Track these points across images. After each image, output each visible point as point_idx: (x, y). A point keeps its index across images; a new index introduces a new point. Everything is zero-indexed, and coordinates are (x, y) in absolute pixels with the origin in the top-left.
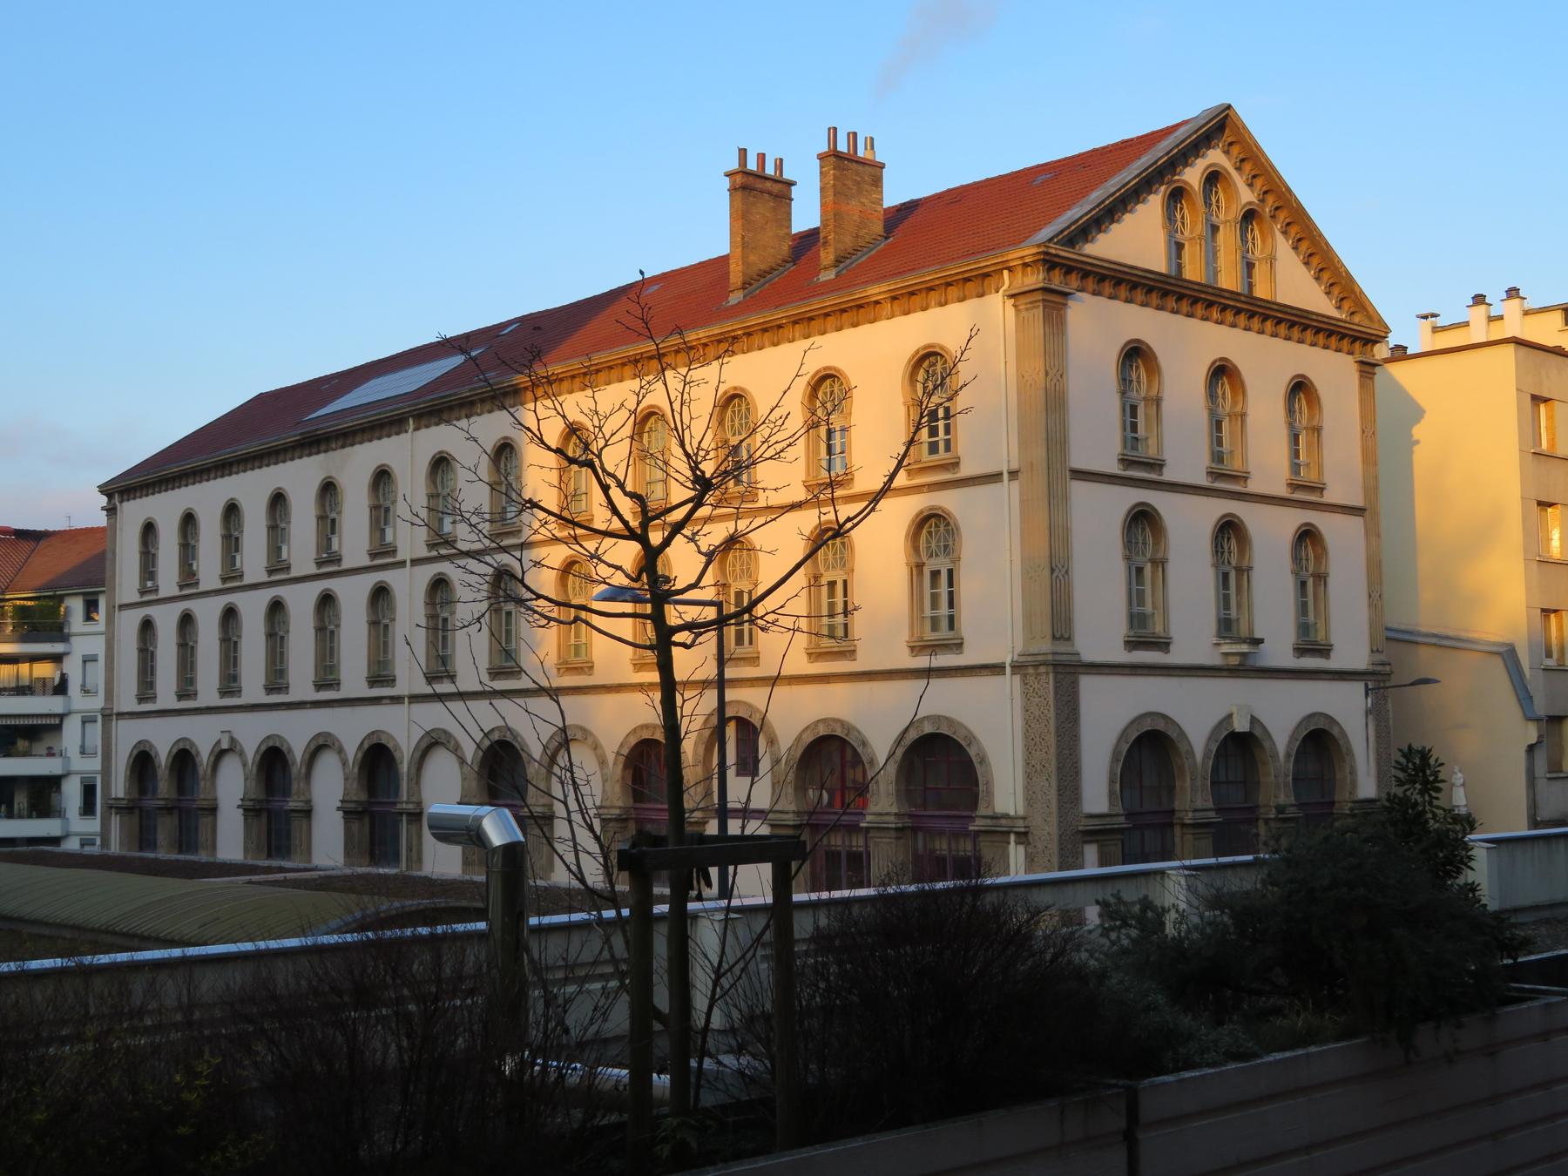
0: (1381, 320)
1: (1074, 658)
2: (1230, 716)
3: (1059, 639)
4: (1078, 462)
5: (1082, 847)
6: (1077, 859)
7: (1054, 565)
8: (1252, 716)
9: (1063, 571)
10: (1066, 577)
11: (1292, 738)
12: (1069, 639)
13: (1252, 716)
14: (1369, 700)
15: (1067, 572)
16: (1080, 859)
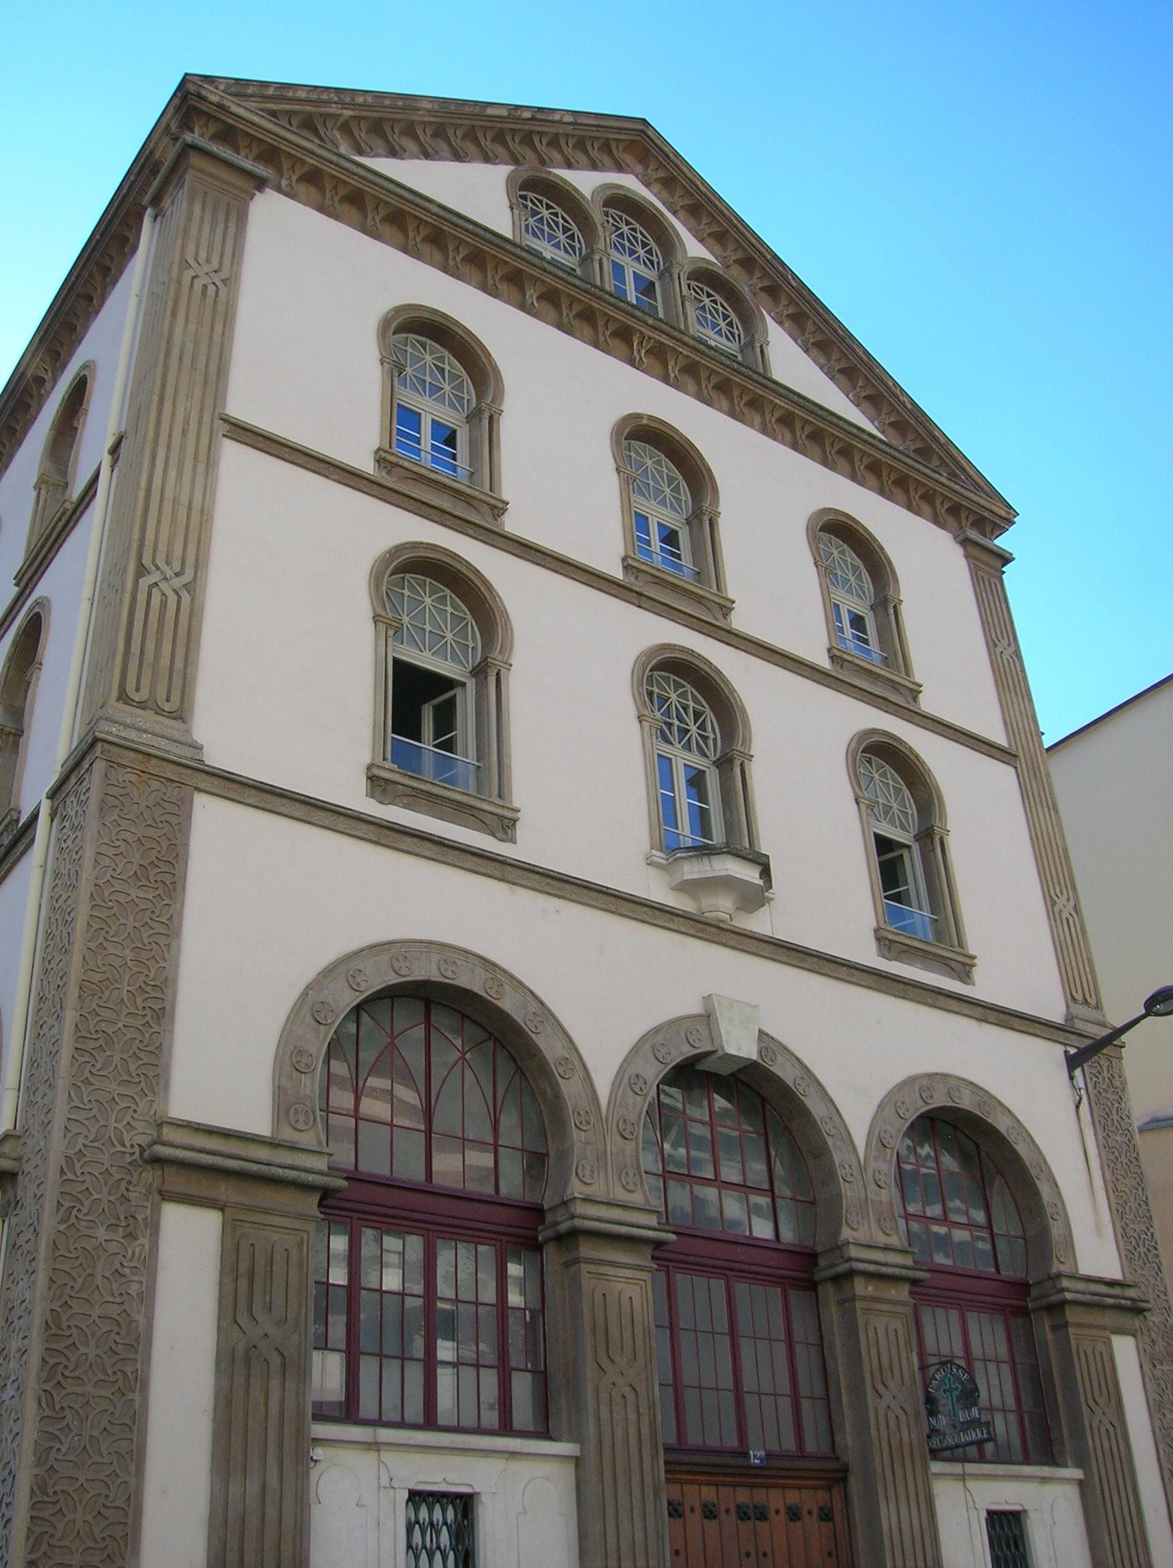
0: (994, 494)
1: (188, 752)
2: (707, 1018)
3: (142, 705)
4: (240, 407)
5: (157, 1211)
6: (132, 1236)
7: (146, 561)
8: (760, 1031)
9: (177, 583)
10: (184, 595)
11: (889, 1102)
12: (181, 715)
13: (760, 1031)
14: (1080, 1082)
15: (190, 587)
16: (144, 1241)
